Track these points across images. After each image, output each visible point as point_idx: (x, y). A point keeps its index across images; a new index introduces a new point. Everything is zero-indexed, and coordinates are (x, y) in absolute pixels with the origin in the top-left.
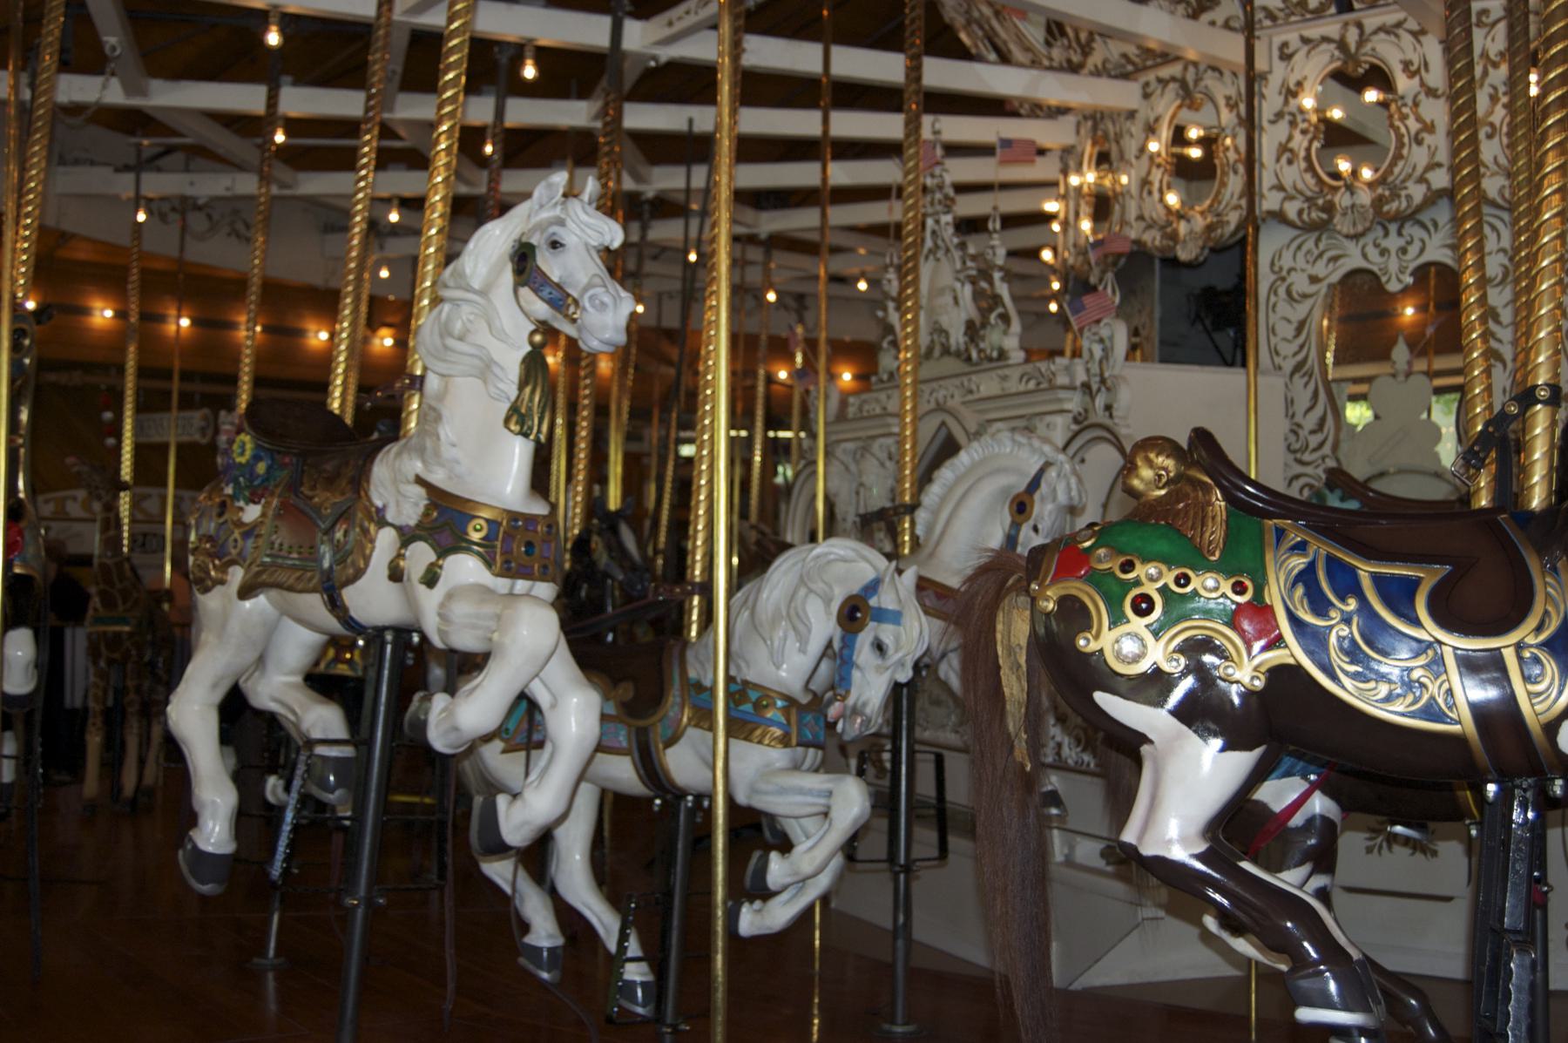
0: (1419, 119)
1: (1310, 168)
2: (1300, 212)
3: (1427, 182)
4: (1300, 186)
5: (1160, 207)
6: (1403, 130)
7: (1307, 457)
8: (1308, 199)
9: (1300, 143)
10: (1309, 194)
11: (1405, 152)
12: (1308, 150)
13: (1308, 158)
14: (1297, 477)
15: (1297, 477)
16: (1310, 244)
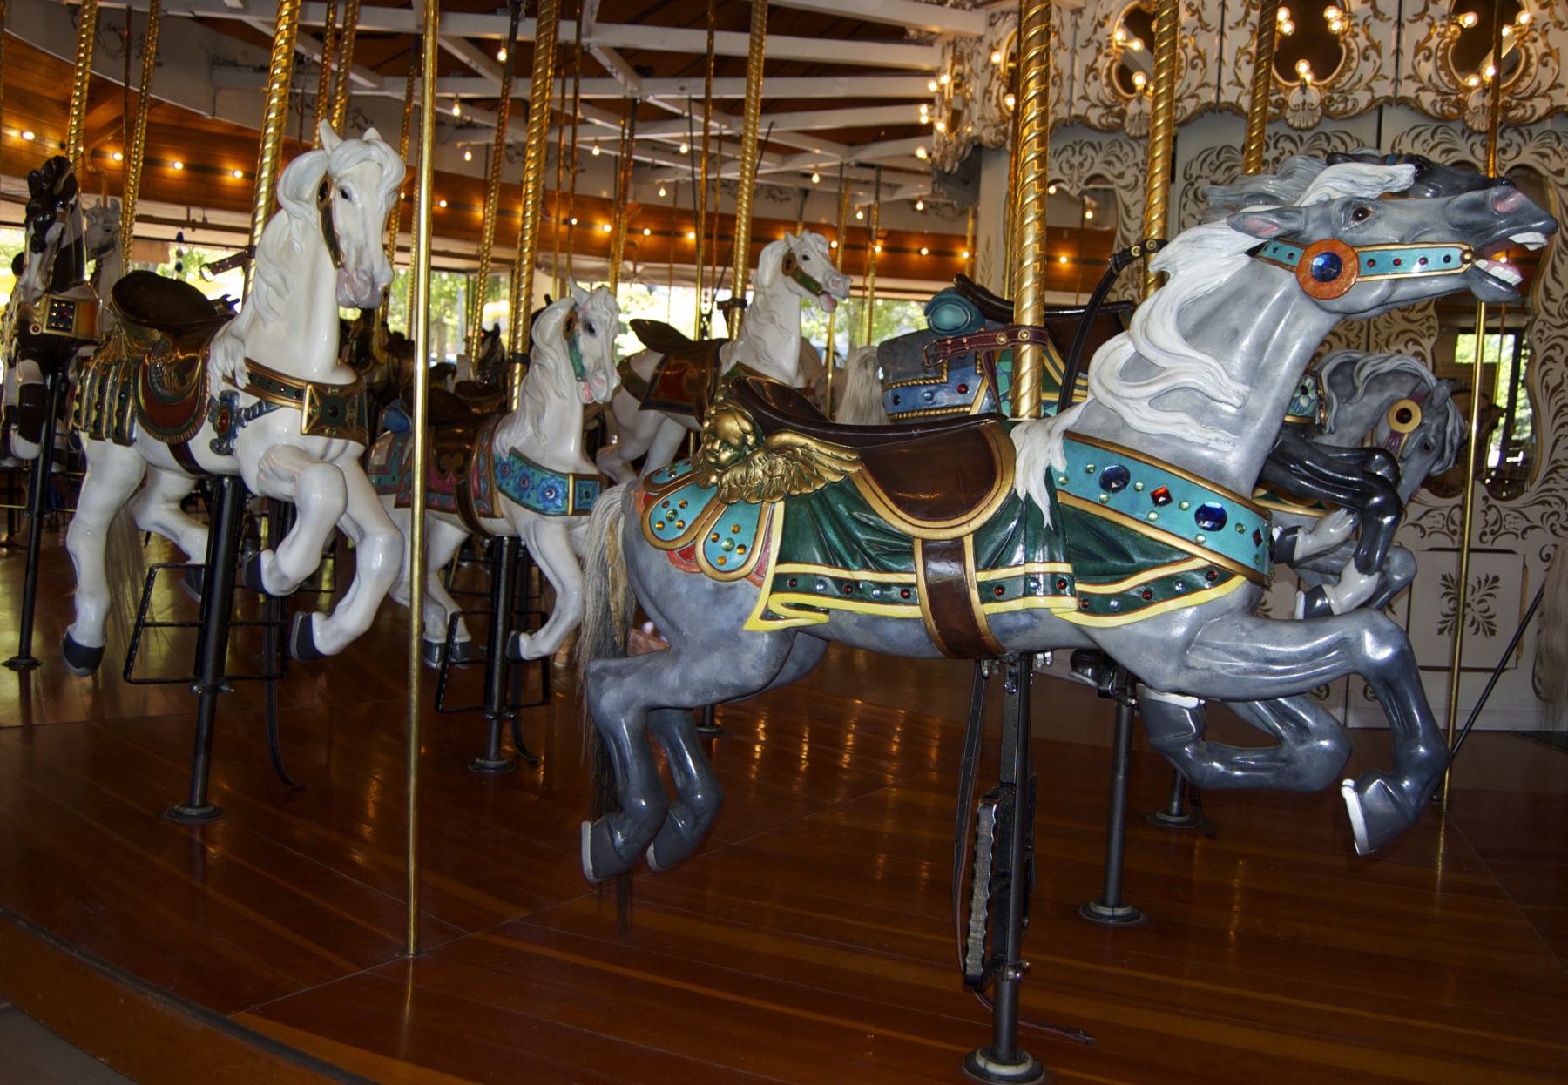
0: (1368, 38)
1: (1110, 84)
2: (1433, 103)
3: (1371, 90)
4: (1435, 80)
5: (996, 111)
6: (1353, 46)
7: (1413, 316)
8: (1107, 107)
9: (1103, 64)
10: (1444, 89)
11: (1354, 65)
12: (1109, 69)
13: (1109, 75)
14: (1404, 332)
15: (1404, 332)
16: (1427, 135)
